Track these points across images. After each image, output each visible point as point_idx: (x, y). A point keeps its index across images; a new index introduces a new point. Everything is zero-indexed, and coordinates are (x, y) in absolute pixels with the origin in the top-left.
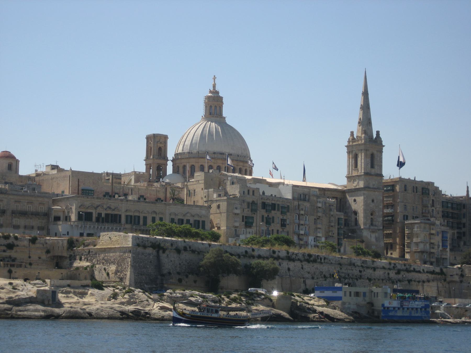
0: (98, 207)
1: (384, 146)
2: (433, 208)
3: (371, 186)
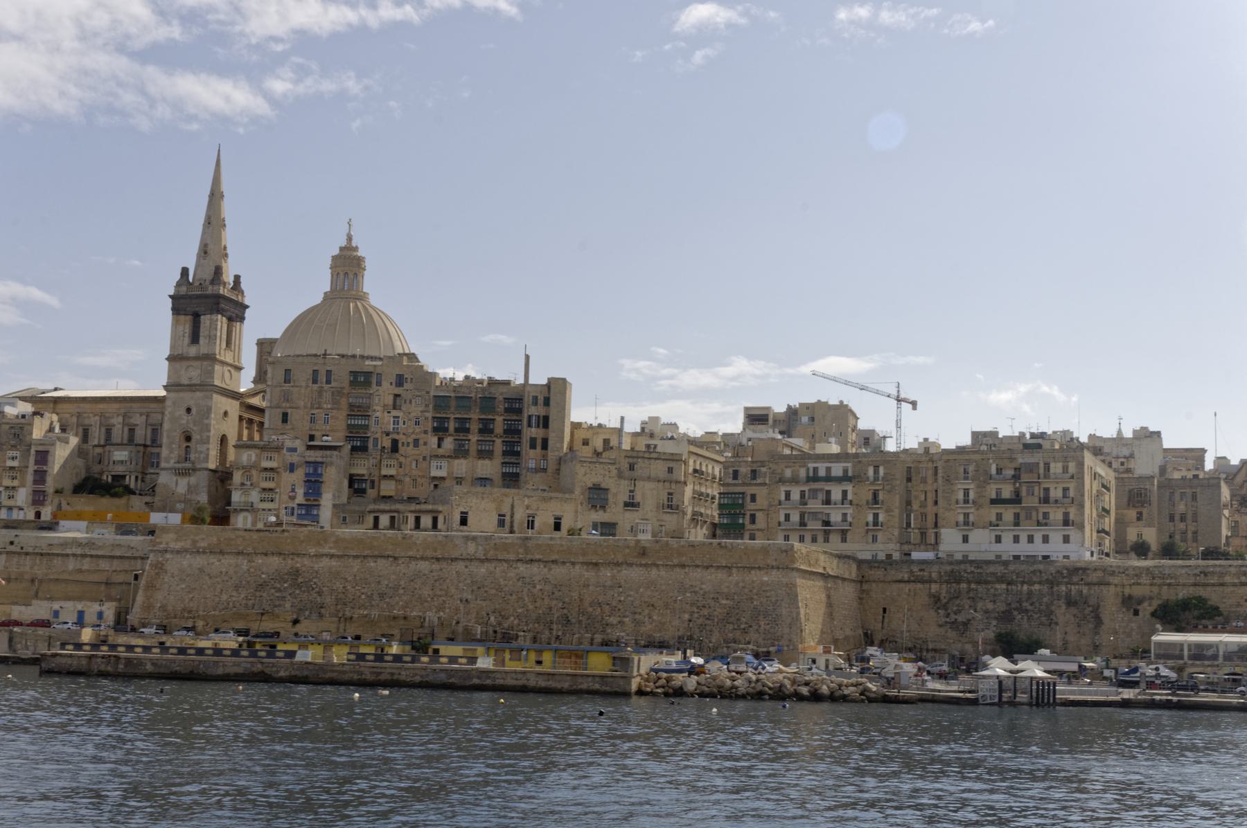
2: (395, 413)
3: (186, 382)
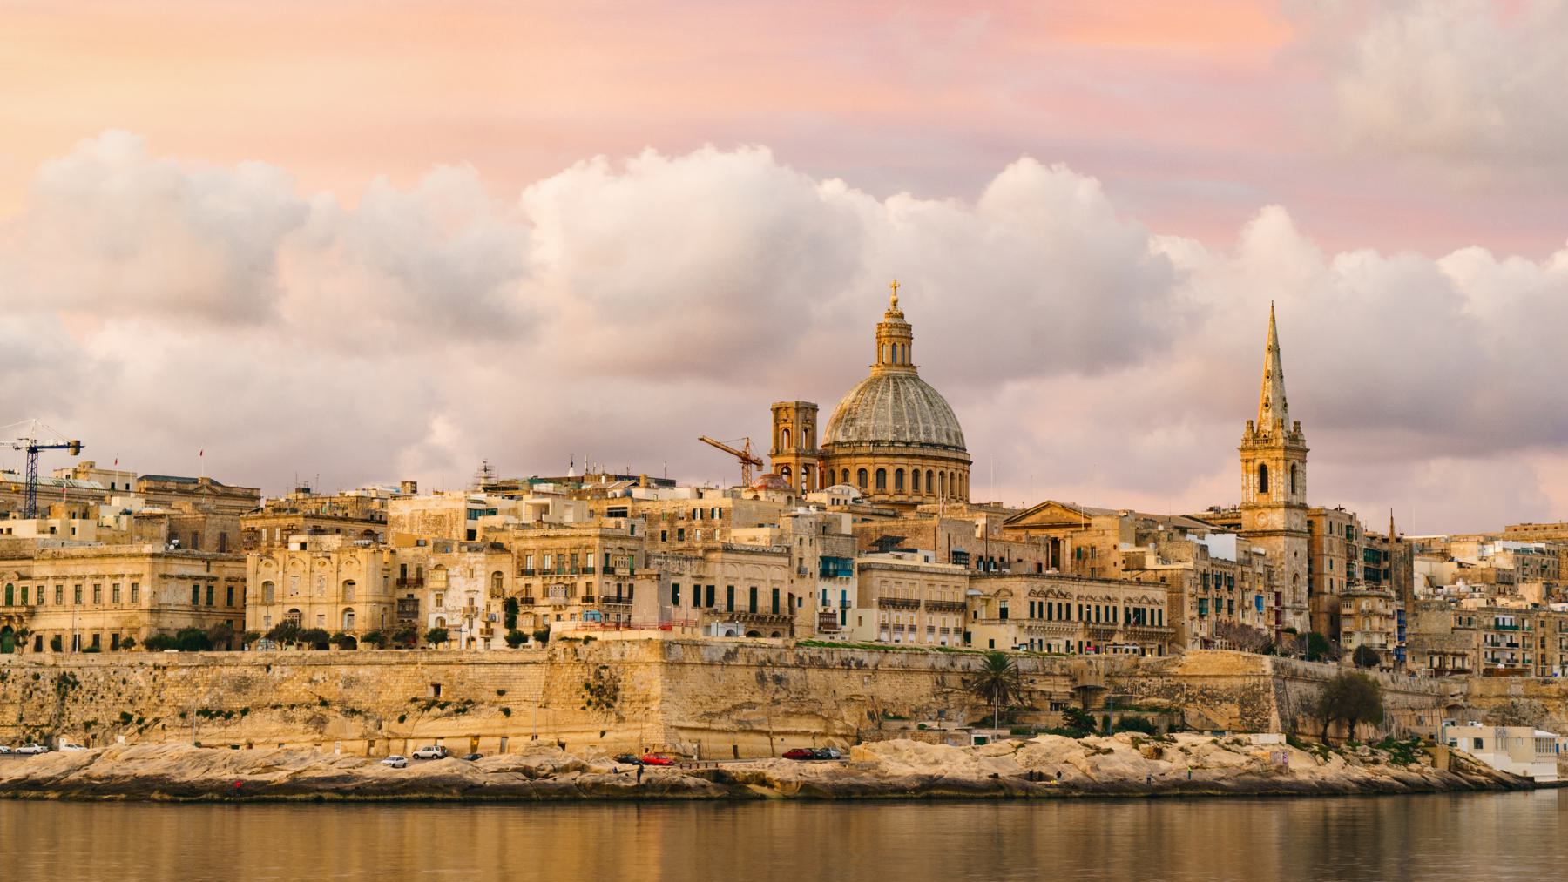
0: (1048, 592)
1: (1308, 450)
